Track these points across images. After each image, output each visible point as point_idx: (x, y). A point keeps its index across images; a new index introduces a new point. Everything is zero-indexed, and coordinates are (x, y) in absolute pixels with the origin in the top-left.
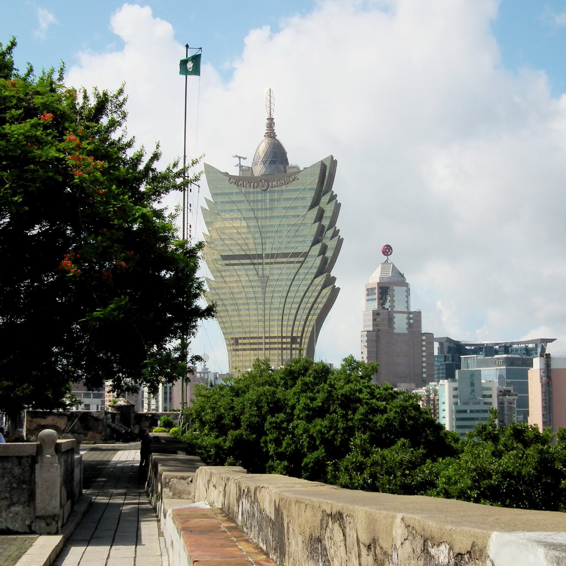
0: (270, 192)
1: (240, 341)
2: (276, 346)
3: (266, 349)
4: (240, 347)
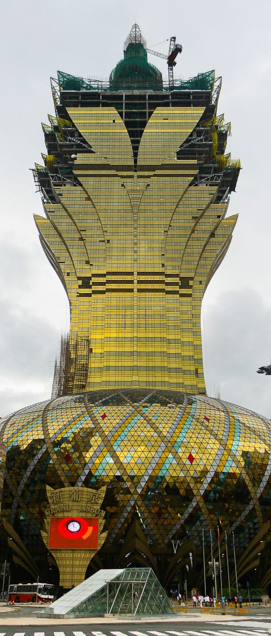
1: (94, 280)
2: (157, 286)
4: (95, 288)
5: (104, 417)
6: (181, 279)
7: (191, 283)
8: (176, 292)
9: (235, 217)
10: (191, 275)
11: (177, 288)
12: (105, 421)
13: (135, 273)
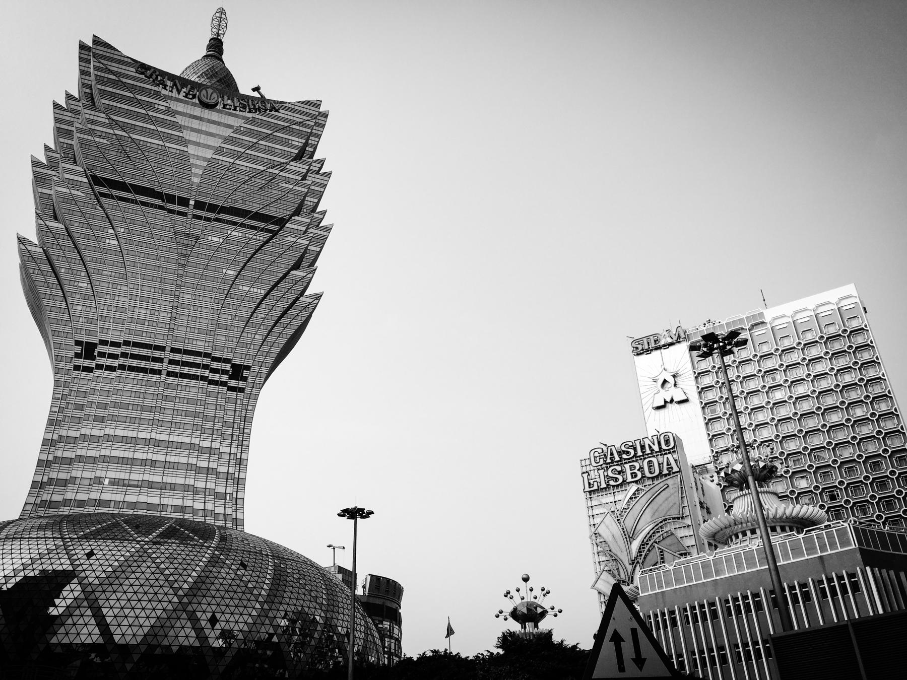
0: (219, 111)
3: (169, 374)
5: (90, 555)
6: (234, 366)
7: (246, 373)
8: (224, 384)
9: (319, 297)
10: (248, 363)
11: (225, 378)
12: (92, 562)
13: (168, 349)
